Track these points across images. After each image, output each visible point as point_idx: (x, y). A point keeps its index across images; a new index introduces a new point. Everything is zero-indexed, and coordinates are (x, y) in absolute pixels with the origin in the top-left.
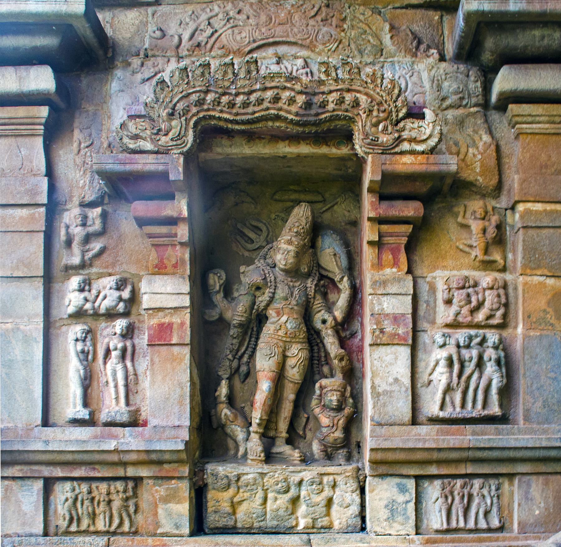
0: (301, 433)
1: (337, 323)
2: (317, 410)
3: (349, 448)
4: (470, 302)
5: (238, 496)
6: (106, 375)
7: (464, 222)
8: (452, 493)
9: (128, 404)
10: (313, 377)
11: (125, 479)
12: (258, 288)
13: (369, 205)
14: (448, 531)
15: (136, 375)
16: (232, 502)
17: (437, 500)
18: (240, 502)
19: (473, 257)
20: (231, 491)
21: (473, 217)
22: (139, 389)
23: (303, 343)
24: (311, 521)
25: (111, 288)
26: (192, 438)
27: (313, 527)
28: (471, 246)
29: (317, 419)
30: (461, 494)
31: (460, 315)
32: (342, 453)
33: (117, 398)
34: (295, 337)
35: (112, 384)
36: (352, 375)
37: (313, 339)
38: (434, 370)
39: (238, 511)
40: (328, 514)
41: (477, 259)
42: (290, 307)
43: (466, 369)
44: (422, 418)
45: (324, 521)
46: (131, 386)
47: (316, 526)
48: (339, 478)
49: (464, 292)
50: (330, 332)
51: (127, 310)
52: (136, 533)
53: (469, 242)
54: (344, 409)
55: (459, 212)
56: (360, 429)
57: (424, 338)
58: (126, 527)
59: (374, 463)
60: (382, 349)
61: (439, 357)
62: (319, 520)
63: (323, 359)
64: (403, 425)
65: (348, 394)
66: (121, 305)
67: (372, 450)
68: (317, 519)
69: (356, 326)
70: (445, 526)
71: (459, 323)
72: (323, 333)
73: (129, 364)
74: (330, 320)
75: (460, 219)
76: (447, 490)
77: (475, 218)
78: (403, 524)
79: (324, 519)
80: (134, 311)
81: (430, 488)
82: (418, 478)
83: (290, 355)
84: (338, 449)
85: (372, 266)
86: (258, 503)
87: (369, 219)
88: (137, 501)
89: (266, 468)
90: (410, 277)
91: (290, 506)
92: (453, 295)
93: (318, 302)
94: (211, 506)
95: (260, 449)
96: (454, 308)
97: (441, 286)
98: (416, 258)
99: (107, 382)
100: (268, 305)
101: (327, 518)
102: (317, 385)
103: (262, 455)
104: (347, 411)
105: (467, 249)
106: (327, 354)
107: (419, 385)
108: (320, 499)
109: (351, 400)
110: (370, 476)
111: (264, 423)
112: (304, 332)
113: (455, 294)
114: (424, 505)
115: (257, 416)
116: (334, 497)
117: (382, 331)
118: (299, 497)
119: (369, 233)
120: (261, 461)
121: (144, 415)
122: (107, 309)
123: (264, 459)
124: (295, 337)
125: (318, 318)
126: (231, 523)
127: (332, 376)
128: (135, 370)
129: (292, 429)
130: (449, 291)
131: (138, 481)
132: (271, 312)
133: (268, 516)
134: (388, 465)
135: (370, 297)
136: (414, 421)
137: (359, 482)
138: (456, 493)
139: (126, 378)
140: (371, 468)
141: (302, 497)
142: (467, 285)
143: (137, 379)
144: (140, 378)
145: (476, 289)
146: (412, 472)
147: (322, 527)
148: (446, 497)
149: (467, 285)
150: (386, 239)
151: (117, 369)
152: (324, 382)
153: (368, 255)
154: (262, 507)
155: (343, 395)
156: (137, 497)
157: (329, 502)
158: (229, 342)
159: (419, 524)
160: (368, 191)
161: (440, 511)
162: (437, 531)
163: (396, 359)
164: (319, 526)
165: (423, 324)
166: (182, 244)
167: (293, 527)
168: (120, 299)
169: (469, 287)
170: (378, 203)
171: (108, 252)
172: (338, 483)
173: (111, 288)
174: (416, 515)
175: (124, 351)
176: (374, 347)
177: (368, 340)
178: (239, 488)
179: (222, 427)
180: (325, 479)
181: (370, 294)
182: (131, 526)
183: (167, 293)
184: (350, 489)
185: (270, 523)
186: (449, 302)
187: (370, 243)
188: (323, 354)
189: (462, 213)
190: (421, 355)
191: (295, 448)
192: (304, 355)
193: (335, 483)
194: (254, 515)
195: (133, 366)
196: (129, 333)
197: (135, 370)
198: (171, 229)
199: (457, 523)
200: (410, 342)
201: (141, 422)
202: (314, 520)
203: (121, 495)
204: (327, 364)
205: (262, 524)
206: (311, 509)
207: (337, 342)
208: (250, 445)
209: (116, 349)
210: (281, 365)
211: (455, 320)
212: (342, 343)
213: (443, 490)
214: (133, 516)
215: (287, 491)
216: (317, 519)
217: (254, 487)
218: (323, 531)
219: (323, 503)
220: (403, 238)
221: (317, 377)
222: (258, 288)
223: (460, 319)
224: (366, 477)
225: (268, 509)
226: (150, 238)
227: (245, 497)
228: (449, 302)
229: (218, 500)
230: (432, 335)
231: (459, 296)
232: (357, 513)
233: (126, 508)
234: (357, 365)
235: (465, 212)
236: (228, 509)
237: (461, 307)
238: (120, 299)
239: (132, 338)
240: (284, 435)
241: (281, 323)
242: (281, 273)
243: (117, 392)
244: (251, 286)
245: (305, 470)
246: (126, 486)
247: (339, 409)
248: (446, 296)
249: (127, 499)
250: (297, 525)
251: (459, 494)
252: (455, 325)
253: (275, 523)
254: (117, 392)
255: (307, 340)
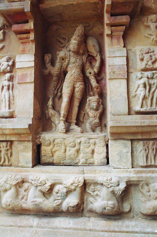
0: (82, 120)
1: (95, 74)
2: (88, 110)
3: (101, 127)
4: (152, 59)
5: (54, 149)
6: (2, 97)
7: (147, 24)
8: (148, 147)
9: (9, 108)
10: (87, 96)
11: (7, 141)
12: (63, 59)
13: (107, 19)
14: (146, 167)
15: (13, 96)
16: (52, 151)
17: (141, 151)
18: (55, 151)
19: (152, 39)
20: (51, 146)
21: (151, 22)
22: (15, 102)
23: (82, 82)
24: (85, 160)
25: (5, 61)
26: (34, 123)
27: (86, 163)
28: (151, 35)
29: (88, 114)
30: (152, 148)
31: (147, 65)
32: (98, 129)
33: (5, 106)
34: (78, 79)
35: (4, 100)
36: (102, 95)
37: (86, 80)
38: (137, 90)
39: (54, 156)
40: (92, 157)
41: (154, 40)
42: (76, 66)
43: (152, 88)
44: (132, 112)
45: (91, 161)
46: (11, 101)
47: (87, 163)
48: (97, 141)
49: (149, 54)
50: (93, 77)
51: (11, 70)
52: (11, 165)
53: (150, 33)
54: (99, 110)
55: (145, 21)
56: (106, 117)
57: (133, 76)
58: (7, 163)
59: (112, 134)
60: (114, 81)
61: (139, 83)
62: (88, 160)
63: (90, 89)
64: (125, 115)
65: (100, 103)
66: (9, 68)
67: (111, 127)
68: (88, 159)
69: (103, 75)
70: (145, 164)
71: (147, 68)
72: (90, 78)
73: (11, 91)
74: (92, 72)
75: (145, 23)
76: (146, 147)
77: (152, 22)
78: (126, 163)
79: (90, 159)
80: (14, 71)
81: (138, 145)
82: (132, 141)
83: (76, 87)
84: (97, 127)
85: (109, 45)
86: (62, 152)
87: (107, 24)
88: (12, 151)
89: (65, 136)
90: (125, 49)
91: (76, 153)
92: (144, 57)
93: (88, 64)
94: (43, 153)
95: (64, 127)
96: (144, 63)
97: (138, 53)
98: (127, 42)
99: (2, 100)
100: (67, 66)
101: (92, 159)
102: (88, 99)
103: (64, 130)
104: (100, 110)
105: (149, 36)
106: (92, 86)
107: (131, 97)
108: (89, 150)
109: (102, 106)
110: (110, 140)
111: (66, 116)
112: (82, 77)
113: (145, 56)
114: (135, 154)
115: (63, 112)
116: (95, 149)
117: (114, 72)
118: (79, 149)
119: (107, 31)
120: (64, 133)
121: (16, 114)
122: (3, 70)
123: (65, 132)
124: (78, 79)
125: (88, 72)
126: (51, 161)
127: (94, 96)
128: (13, 94)
129: (78, 119)
130: (142, 55)
131: (12, 142)
132: (69, 69)
133: (67, 158)
134: (118, 135)
135: (108, 58)
136: (129, 114)
137: (106, 142)
138: (150, 147)
139: (9, 98)
140: (111, 136)
141: (81, 149)
142: (150, 51)
143: (14, 98)
144: (15, 98)
145: (154, 53)
146: (129, 138)
147: (90, 163)
148: (146, 150)
149: (150, 51)
150: (114, 33)
151: (5, 94)
152: (90, 98)
153: (107, 40)
154: (64, 154)
155: (98, 103)
156: (12, 149)
157: (93, 152)
158: (53, 84)
159: (133, 163)
160: (106, 12)
161: (143, 157)
162: (142, 167)
163: (120, 85)
164: (89, 163)
165: (131, 70)
166: (32, 41)
167: (77, 163)
168: (8, 65)
169: (151, 52)
170: (110, 17)
171: (5, 48)
172: (96, 143)
173: (5, 61)
174: (132, 158)
175: (9, 86)
176: (111, 80)
177: (108, 77)
178: (54, 145)
179: (49, 119)
180: (91, 141)
181: (108, 57)
182: (9, 162)
183: (26, 60)
184: (102, 145)
185: (67, 161)
186: (142, 60)
187: (108, 35)
188: (90, 87)
189: (146, 21)
190: (131, 83)
191: (79, 127)
192: (82, 86)
193: (95, 142)
194: (61, 158)
195: (13, 93)
196: (11, 79)
197: (13, 94)
198: (28, 35)
199: (151, 162)
200: (126, 77)
201: (15, 116)
202: (86, 160)
203: (5, 148)
204: (92, 91)
205: (64, 161)
206: (85, 155)
207: (95, 81)
208: (59, 125)
209: (5, 86)
210: (73, 91)
211: (145, 67)
212: (98, 82)
213: (144, 146)
214: (10, 158)
215: (74, 146)
216: (88, 159)
217: (61, 145)
218: (90, 165)
219: (91, 152)
220: (122, 32)
221: (88, 96)
222: (63, 59)
223: (147, 67)
224: (108, 140)
225: (67, 155)
226: (20, 40)
227: (57, 149)
228: (142, 60)
229: (45, 150)
230: (136, 75)
231: (147, 57)
232: (105, 157)
233: (7, 154)
234: (104, 91)
235: (147, 20)
236: (51, 155)
237: (148, 61)
238: (8, 65)
239: (12, 81)
240: (75, 121)
241: (73, 73)
242: (72, 53)
243: (5, 104)
244: (60, 58)
245: (82, 137)
246: (7, 144)
247: (97, 110)
248: (141, 57)
249: (7, 150)
250: (79, 162)
251: (151, 148)
252: (145, 70)
253: (70, 161)
254: (5, 104)
255: (83, 81)
